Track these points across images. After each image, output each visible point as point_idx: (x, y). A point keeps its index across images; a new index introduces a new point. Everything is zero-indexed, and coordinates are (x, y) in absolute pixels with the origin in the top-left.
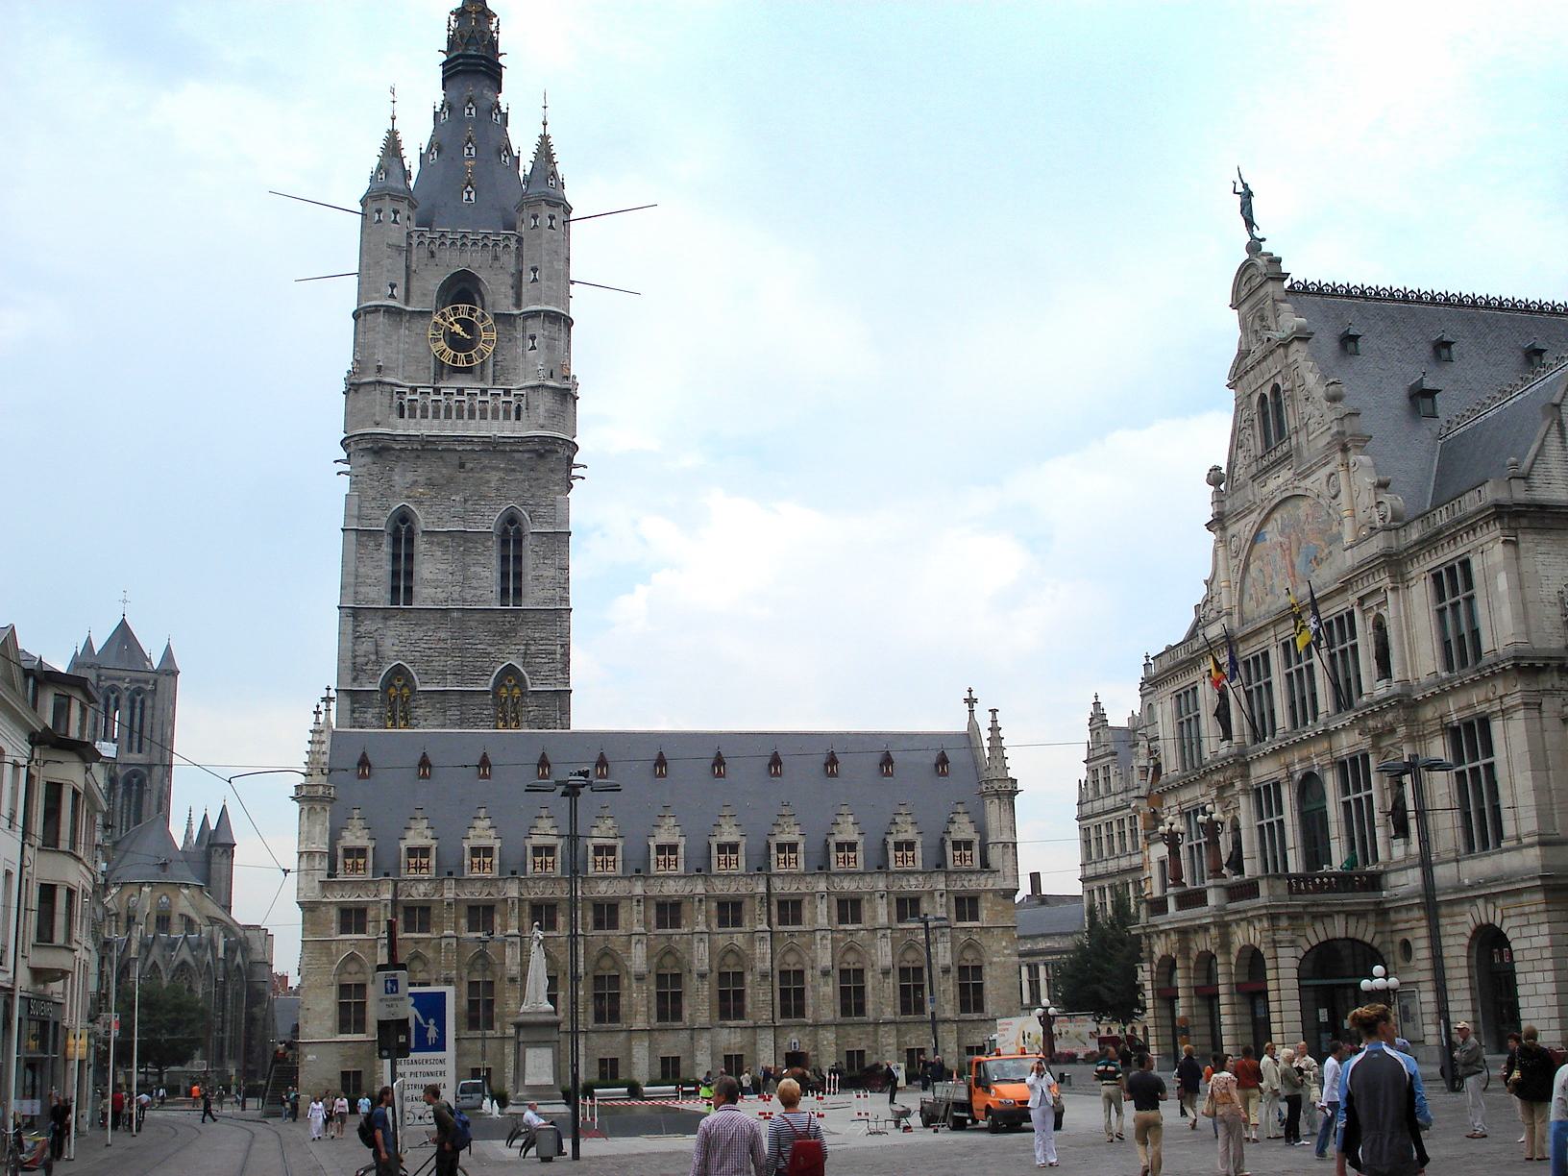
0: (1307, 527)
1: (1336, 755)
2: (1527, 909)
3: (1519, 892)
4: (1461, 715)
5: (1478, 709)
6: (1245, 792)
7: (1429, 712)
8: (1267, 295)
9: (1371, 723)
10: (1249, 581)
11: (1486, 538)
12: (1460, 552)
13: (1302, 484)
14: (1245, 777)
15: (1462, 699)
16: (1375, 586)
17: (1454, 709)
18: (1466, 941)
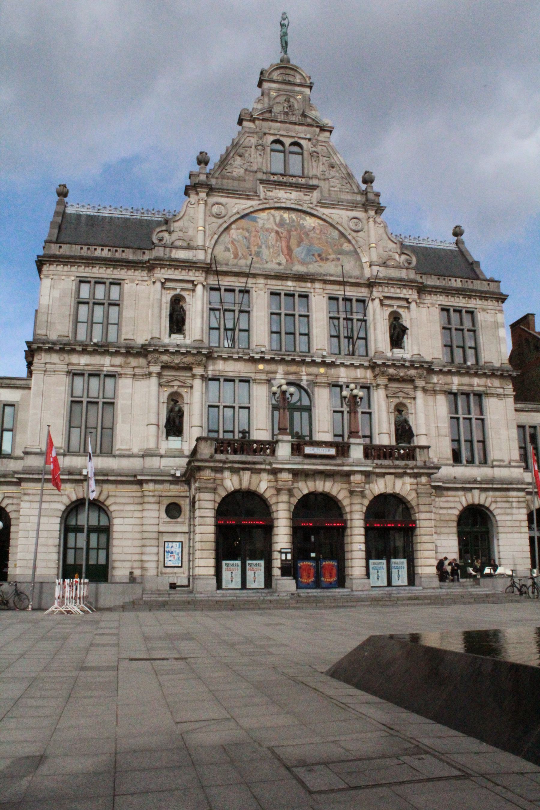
0: (312, 234)
1: (334, 379)
2: (510, 499)
3: (508, 490)
4: (461, 388)
5: (476, 389)
6: (203, 377)
7: (435, 379)
8: (301, 93)
9: (391, 371)
10: (225, 238)
11: (492, 308)
12: (468, 306)
13: (318, 208)
14: (205, 368)
15: (466, 380)
16: (402, 296)
17: (456, 383)
18: (457, 512)
